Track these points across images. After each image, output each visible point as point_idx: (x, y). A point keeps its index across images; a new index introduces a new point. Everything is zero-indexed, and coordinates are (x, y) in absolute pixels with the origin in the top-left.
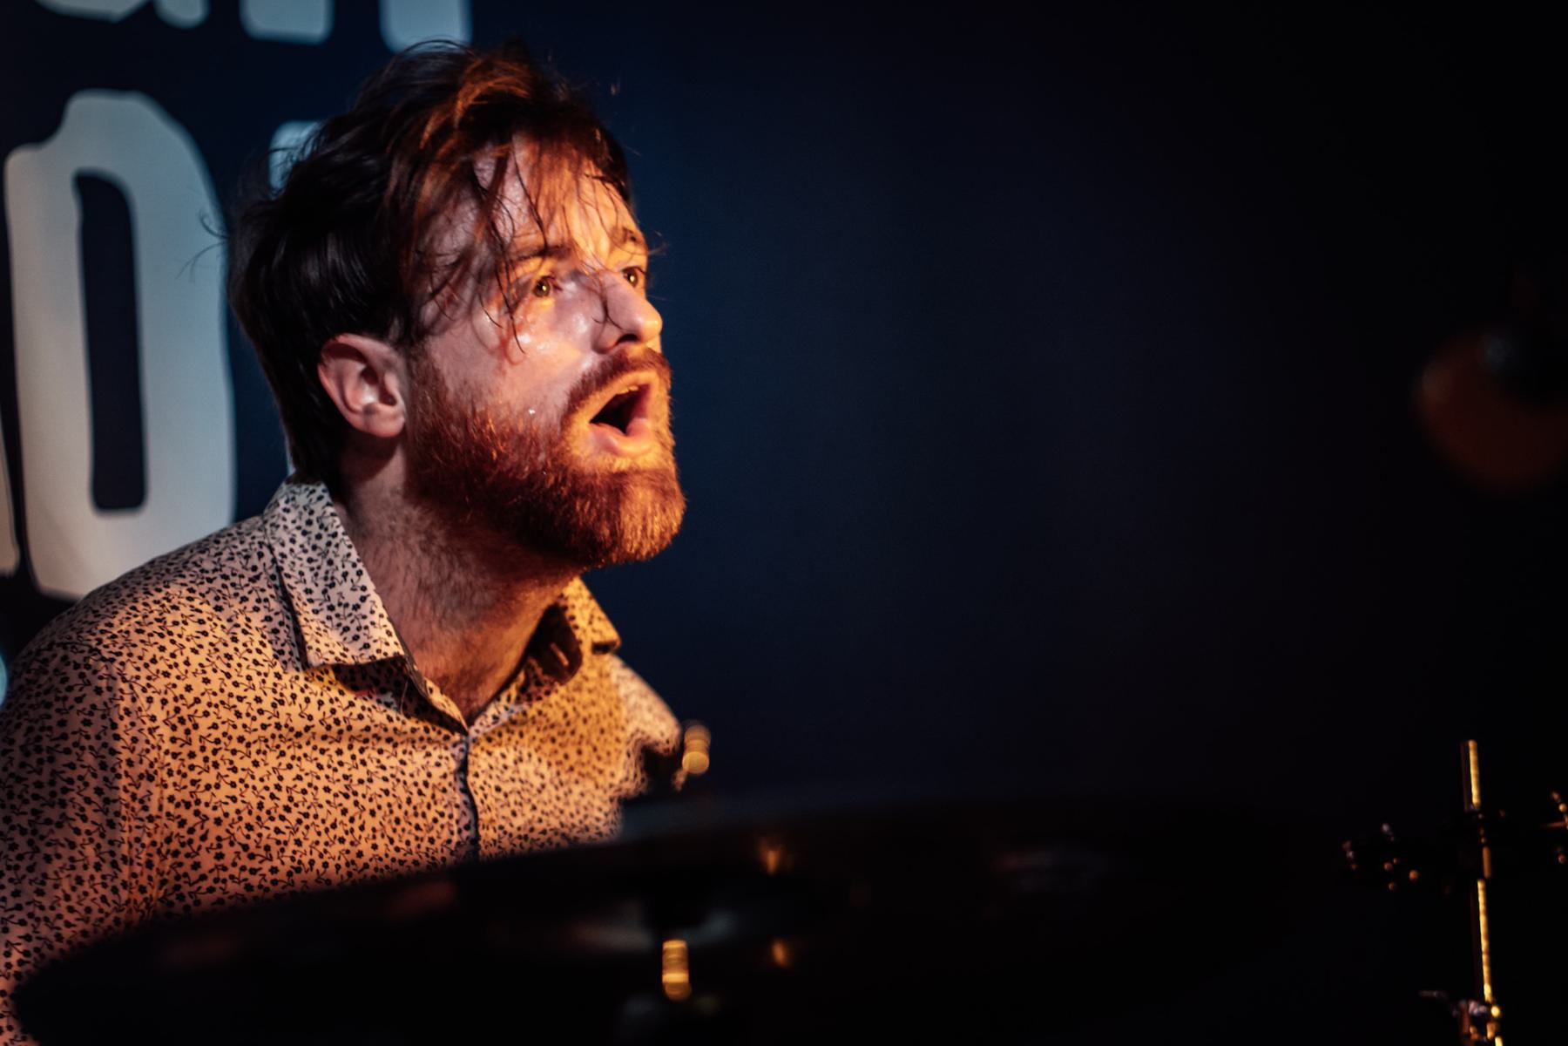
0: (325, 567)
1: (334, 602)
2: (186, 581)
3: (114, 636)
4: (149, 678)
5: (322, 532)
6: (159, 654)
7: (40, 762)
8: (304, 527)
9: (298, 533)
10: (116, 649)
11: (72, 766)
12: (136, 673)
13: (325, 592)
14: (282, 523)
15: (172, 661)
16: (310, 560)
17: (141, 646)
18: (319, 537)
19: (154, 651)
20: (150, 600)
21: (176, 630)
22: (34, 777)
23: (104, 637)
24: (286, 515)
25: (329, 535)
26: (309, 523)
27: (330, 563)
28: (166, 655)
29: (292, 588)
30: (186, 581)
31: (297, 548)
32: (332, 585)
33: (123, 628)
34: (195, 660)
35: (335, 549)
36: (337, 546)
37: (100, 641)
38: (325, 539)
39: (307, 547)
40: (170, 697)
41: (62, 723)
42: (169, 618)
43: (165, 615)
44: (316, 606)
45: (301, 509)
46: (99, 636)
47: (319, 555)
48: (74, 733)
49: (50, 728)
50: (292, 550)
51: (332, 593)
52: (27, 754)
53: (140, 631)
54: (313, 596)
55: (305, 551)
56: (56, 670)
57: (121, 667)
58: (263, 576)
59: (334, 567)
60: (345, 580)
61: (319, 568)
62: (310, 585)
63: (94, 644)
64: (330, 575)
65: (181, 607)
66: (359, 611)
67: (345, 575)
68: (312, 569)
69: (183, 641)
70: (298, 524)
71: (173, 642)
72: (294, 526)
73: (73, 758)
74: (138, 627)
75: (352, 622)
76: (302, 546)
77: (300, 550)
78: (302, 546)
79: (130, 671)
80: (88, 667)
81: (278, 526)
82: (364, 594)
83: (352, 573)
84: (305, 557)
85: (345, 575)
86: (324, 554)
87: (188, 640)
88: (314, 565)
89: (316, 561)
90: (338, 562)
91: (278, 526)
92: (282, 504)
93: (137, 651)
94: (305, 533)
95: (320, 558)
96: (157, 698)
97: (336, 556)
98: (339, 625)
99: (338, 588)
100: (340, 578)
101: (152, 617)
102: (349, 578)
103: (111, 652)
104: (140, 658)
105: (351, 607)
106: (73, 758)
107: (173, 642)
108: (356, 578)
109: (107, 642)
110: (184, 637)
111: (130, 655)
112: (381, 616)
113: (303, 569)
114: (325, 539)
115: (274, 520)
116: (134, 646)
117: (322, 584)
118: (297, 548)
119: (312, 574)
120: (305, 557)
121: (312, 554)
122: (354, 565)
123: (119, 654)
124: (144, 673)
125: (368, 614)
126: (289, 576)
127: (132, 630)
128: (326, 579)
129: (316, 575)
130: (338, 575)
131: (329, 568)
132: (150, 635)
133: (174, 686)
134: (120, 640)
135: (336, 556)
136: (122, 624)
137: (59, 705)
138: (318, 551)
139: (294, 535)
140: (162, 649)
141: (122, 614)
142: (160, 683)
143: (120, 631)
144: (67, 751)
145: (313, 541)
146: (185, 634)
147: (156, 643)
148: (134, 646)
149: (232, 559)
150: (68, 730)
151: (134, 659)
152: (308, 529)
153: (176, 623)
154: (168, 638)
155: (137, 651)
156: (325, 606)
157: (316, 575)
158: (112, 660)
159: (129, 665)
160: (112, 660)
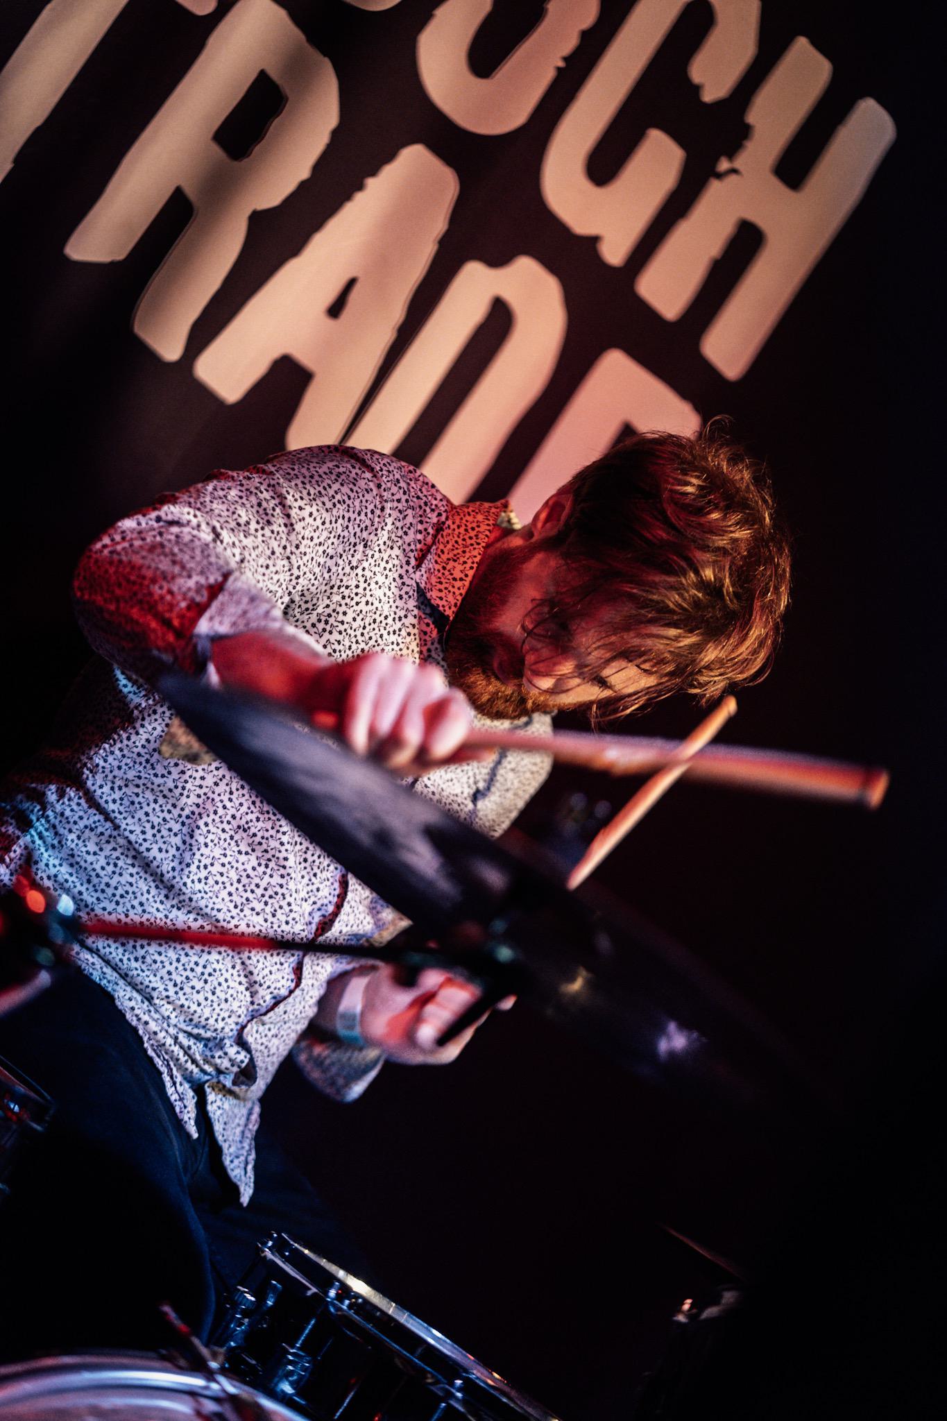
68: (453, 546)
98: (440, 578)
118: (456, 532)
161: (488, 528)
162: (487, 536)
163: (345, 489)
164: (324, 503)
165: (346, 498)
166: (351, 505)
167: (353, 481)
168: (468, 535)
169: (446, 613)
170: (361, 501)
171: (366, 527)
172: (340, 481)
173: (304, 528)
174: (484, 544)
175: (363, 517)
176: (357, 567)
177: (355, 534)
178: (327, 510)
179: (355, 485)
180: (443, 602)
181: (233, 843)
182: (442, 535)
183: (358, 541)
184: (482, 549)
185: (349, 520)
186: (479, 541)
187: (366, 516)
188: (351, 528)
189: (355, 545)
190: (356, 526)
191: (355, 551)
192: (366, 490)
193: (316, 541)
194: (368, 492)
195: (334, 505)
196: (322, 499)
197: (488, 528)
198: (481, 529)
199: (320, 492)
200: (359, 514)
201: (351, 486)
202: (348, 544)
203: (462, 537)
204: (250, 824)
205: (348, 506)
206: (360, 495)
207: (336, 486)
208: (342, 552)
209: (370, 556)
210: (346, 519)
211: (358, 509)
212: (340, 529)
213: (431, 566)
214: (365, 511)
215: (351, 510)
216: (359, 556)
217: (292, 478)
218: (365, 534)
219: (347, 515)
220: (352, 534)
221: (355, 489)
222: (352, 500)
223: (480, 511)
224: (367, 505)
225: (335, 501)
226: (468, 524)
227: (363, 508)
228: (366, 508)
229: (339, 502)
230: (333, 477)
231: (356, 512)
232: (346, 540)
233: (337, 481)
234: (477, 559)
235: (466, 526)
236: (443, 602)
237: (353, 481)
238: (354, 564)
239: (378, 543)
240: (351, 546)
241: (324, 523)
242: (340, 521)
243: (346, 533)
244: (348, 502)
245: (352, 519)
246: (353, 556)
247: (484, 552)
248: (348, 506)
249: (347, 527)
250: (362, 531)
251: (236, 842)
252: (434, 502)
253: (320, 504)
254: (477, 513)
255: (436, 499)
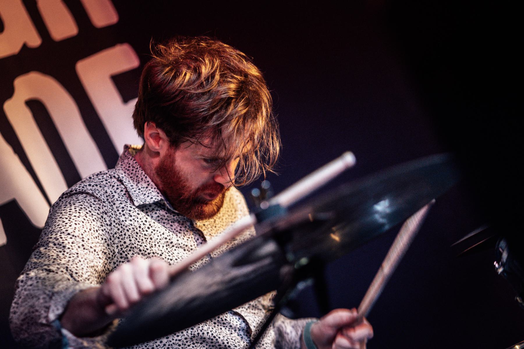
0: (136, 178)
8: (128, 168)
16: (131, 177)
25: (136, 169)
29: (127, 185)
31: (126, 175)
36: (138, 171)
47: (133, 175)
50: (125, 175)
55: (129, 175)
59: (138, 177)
60: (142, 180)
61: (134, 179)
68: (132, 180)
83: (144, 178)
88: (132, 178)
89: (133, 177)
95: (134, 176)
97: (138, 174)
108: (145, 179)
113: (129, 180)
119: (132, 181)
121: (132, 176)
122: (144, 176)
126: (125, 182)
128: (136, 181)
129: (133, 181)
131: (137, 178)
135: (138, 174)
139: (125, 171)
145: (131, 172)
157: (133, 181)
161: (133, 160)
162: (136, 163)
163: (77, 204)
164: (75, 216)
165: (81, 207)
166: (85, 207)
167: (76, 199)
168: (131, 170)
169: (159, 199)
170: (87, 202)
171: (99, 208)
172: (72, 204)
173: (79, 231)
174: (139, 167)
175: (93, 206)
176: (111, 223)
177: (98, 214)
178: (79, 217)
179: (79, 200)
180: (154, 198)
181: (196, 344)
182: (124, 182)
183: (101, 215)
184: (140, 168)
185: (90, 212)
186: (136, 167)
187: (94, 204)
188: (94, 214)
189: (102, 217)
190: (95, 211)
191: (105, 219)
192: (84, 198)
193: (88, 230)
194: (86, 198)
195: (79, 213)
196: (73, 215)
197: (133, 160)
198: (131, 163)
199: (69, 214)
200: (91, 206)
201: (78, 201)
202: (99, 219)
203: (130, 174)
204: (193, 333)
205: (84, 208)
206: (84, 201)
207: (73, 207)
208: (101, 224)
209: (111, 215)
210: (89, 213)
211: (89, 205)
212: (91, 218)
213: (135, 195)
214: (92, 203)
215: (87, 208)
216: (107, 219)
217: (55, 221)
218: (101, 210)
219: (87, 211)
220: (97, 215)
221: (80, 201)
222: (83, 205)
223: (123, 160)
224: (90, 201)
225: (78, 211)
226: (126, 168)
227: (90, 203)
228: (91, 202)
229: (80, 210)
230: (69, 206)
231: (89, 207)
232: (97, 219)
233: (71, 205)
234: (144, 173)
235: (126, 169)
236: (154, 198)
237: (76, 199)
238: (109, 223)
239: (109, 208)
240: (102, 219)
241: (83, 222)
242: (87, 215)
243: (94, 217)
244: (82, 207)
245: (91, 210)
246: (106, 221)
247: (142, 168)
248: (84, 208)
249: (92, 214)
250: (99, 210)
251: (196, 343)
252: (108, 175)
253: (74, 218)
254: (123, 161)
255: (107, 173)
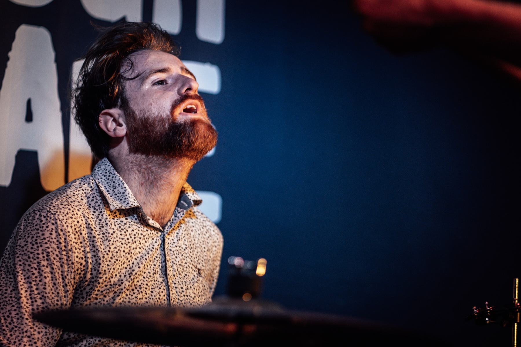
0: (112, 184)
1: (116, 193)
2: (72, 190)
3: (54, 207)
4: (67, 219)
5: (110, 174)
6: (69, 211)
7: (38, 247)
9: (103, 176)
10: (56, 210)
11: (48, 248)
12: (62, 218)
13: (113, 191)
14: (97, 174)
15: (73, 213)
17: (63, 209)
18: (109, 176)
19: (67, 210)
20: (62, 196)
21: (72, 204)
22: (37, 252)
23: (51, 207)
24: (98, 172)
26: (106, 173)
27: (114, 182)
28: (71, 211)
30: (72, 190)
32: (115, 188)
33: (57, 203)
34: (79, 213)
35: (115, 178)
36: (116, 177)
37: (50, 208)
38: (111, 176)
39: (106, 180)
40: (73, 225)
41: (43, 235)
42: (69, 201)
43: (68, 200)
44: (111, 195)
45: (103, 170)
46: (49, 206)
48: (48, 237)
49: (39, 236)
51: (116, 191)
52: (33, 245)
53: (62, 204)
54: (110, 192)
55: (106, 181)
56: (38, 219)
57: (58, 216)
58: (94, 189)
59: (115, 183)
61: (110, 184)
62: (109, 190)
63: (48, 209)
64: (114, 186)
65: (72, 198)
66: (125, 194)
67: (119, 185)
69: (75, 207)
70: (102, 174)
71: (72, 207)
72: (101, 175)
73: (48, 245)
74: (61, 203)
75: (123, 197)
76: (104, 180)
77: (104, 181)
78: (104, 180)
79: (61, 218)
80: (48, 217)
81: (96, 175)
82: (126, 189)
84: (106, 182)
85: (119, 185)
86: (112, 180)
87: (76, 207)
88: (109, 184)
90: (116, 182)
91: (96, 175)
92: (97, 169)
93: (62, 211)
94: (105, 176)
96: (69, 226)
97: (115, 180)
99: (117, 189)
100: (118, 186)
101: (64, 200)
102: (120, 185)
103: (54, 211)
104: (63, 213)
105: (122, 193)
106: (48, 245)
107: (72, 207)
109: (52, 208)
110: (75, 206)
111: (60, 212)
112: (131, 195)
114: (111, 176)
115: (95, 174)
116: (61, 209)
117: (112, 189)
119: (109, 186)
120: (106, 182)
121: (108, 181)
123: (57, 212)
124: (65, 218)
125: (127, 194)
127: (59, 204)
129: (110, 186)
130: (117, 185)
131: (114, 184)
132: (65, 205)
133: (74, 221)
134: (56, 207)
135: (115, 180)
136: (55, 202)
137: (41, 229)
138: (110, 180)
140: (69, 209)
141: (55, 200)
142: (70, 221)
143: (56, 205)
144: (46, 243)
145: (108, 177)
146: (75, 205)
147: (67, 208)
148: (61, 209)
149: (84, 184)
150: (45, 236)
151: (62, 213)
152: (106, 174)
153: (72, 202)
154: (70, 206)
155: (62, 211)
156: (114, 194)
157: (110, 186)
158: (55, 214)
159: (60, 215)
160: (55, 214)
